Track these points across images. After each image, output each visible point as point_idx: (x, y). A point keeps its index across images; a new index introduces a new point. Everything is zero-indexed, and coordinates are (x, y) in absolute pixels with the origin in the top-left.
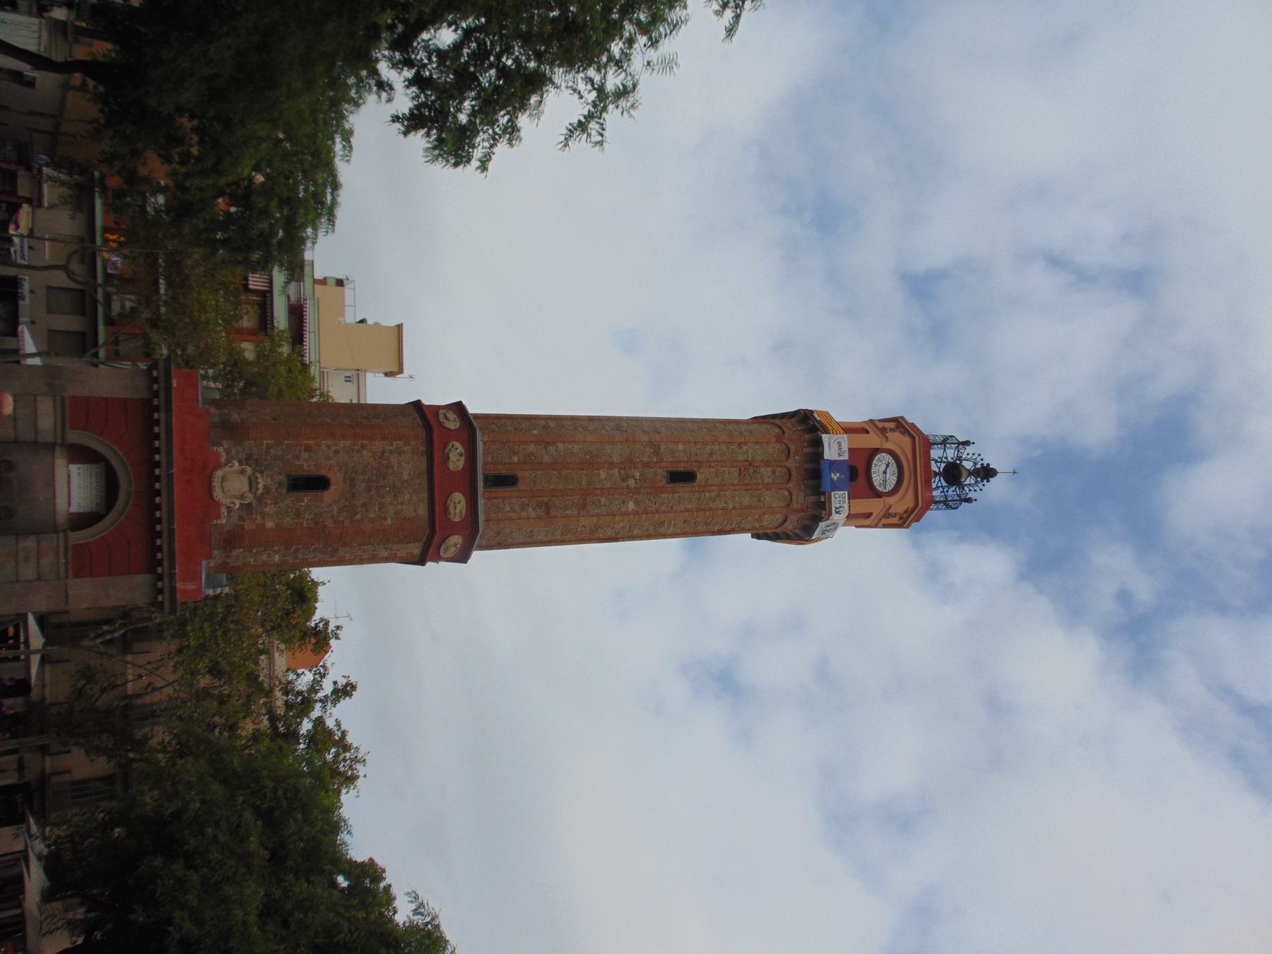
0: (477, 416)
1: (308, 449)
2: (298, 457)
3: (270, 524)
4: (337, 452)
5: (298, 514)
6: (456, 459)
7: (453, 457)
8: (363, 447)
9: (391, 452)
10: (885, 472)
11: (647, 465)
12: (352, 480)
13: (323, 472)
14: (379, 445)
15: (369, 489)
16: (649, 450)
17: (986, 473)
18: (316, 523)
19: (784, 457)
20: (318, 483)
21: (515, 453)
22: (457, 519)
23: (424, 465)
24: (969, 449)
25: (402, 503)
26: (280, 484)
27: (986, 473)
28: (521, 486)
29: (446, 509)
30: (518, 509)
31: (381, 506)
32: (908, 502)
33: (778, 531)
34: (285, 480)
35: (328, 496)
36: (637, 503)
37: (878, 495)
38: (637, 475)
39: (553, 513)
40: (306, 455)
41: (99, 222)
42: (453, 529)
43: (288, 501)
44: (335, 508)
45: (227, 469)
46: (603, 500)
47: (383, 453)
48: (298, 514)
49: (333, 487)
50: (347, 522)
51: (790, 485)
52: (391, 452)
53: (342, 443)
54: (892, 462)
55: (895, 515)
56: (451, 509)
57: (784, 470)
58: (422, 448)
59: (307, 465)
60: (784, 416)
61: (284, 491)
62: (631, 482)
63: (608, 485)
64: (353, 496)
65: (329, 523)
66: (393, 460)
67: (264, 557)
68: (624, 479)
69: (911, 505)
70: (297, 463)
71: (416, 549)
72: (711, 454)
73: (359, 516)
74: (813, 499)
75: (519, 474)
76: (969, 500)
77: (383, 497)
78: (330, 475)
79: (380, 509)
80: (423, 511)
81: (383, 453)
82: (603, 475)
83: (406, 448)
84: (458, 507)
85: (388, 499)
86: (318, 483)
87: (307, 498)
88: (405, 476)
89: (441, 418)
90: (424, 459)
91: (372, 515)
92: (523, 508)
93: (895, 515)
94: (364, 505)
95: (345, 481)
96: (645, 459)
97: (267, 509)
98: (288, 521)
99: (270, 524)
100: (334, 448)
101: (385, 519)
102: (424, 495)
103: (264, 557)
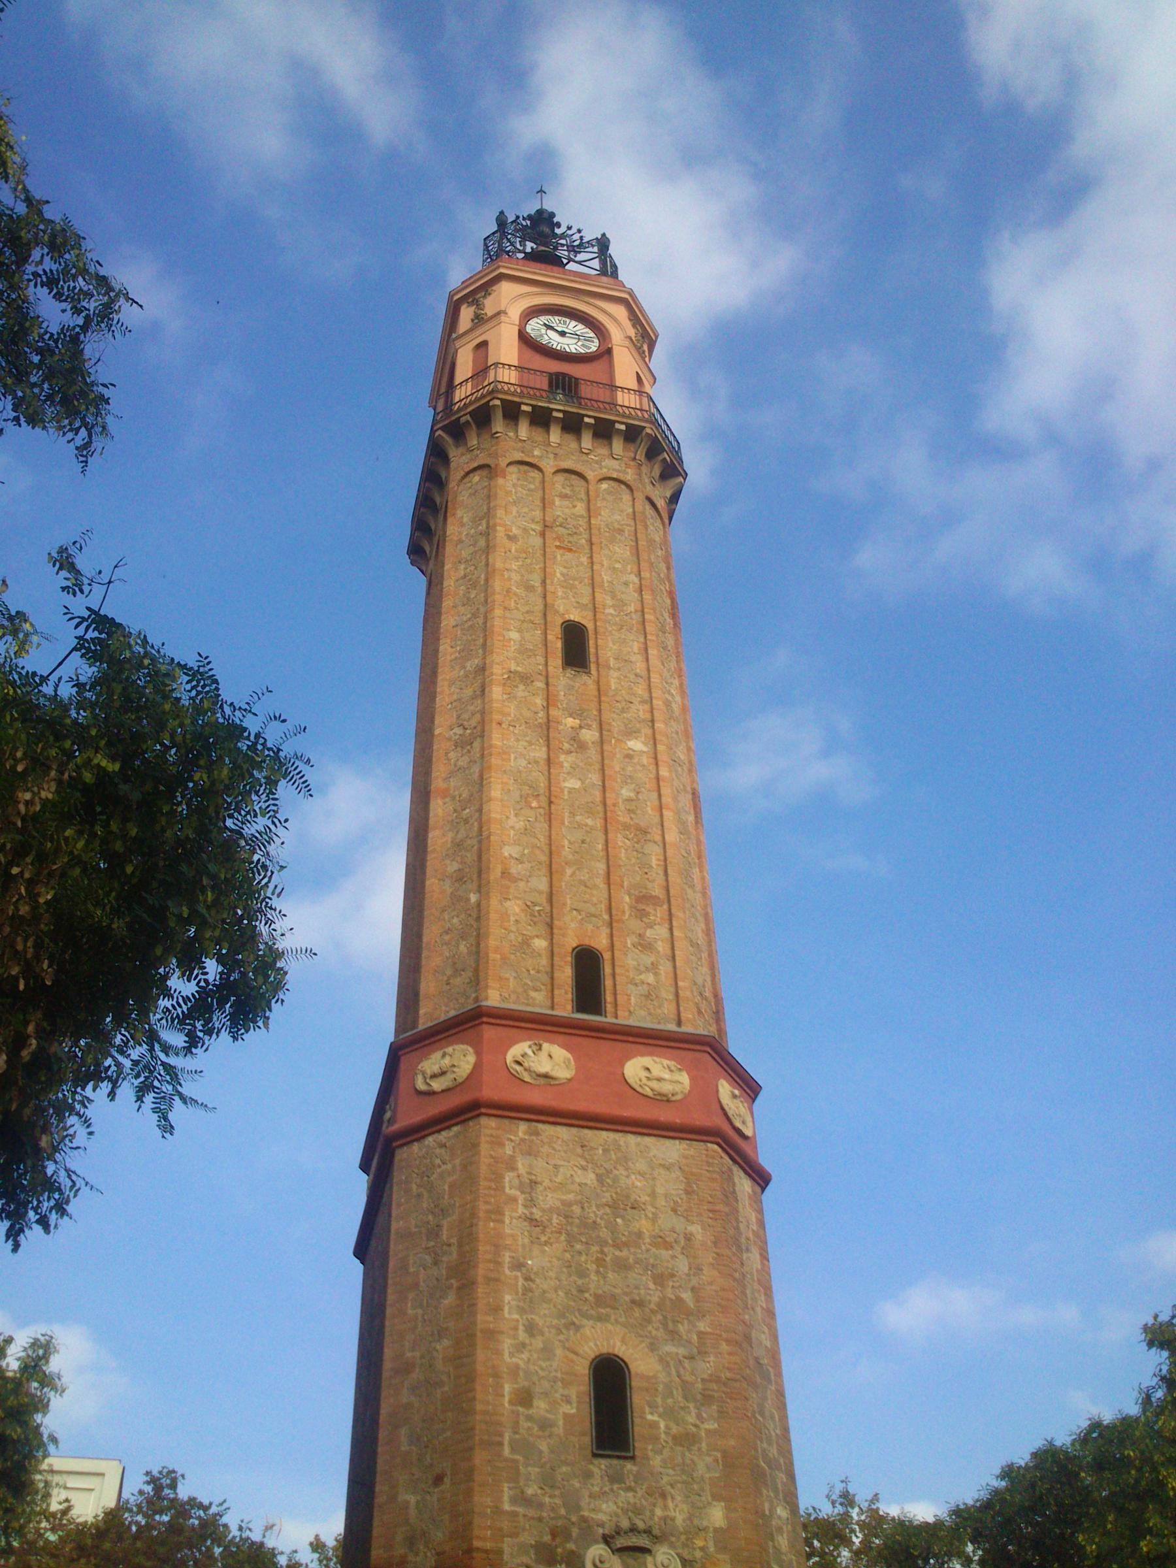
1: (524, 1398)
2: (545, 1425)
3: (717, 1516)
4: (531, 1329)
6: (552, 1060)
7: (544, 1066)
8: (518, 1265)
9: (531, 1202)
10: (563, 334)
11: (549, 701)
12: (600, 1300)
13: (583, 1369)
14: (512, 1225)
15: (622, 1266)
16: (521, 691)
18: (707, 1399)
19: (535, 474)
21: (526, 942)
22: (685, 1078)
23: (563, 1132)
25: (653, 1194)
26: (615, 1478)
28: (600, 942)
29: (663, 1099)
30: (648, 959)
31: (661, 1242)
32: (620, 312)
34: (604, 1463)
35: (642, 1364)
36: (631, 733)
37: (606, 353)
38: (570, 722)
39: (657, 891)
40: (540, 1406)
42: (704, 1092)
43: (656, 1462)
44: (669, 1348)
46: (626, 793)
47: (532, 1221)
48: (687, 1440)
49: (620, 1349)
50: (702, 1326)
51: (590, 475)
52: (531, 1202)
53: (510, 1314)
54: (544, 319)
56: (666, 1088)
57: (560, 478)
58: (523, 1127)
59: (570, 1405)
61: (629, 1466)
62: (589, 735)
63: (595, 778)
64: (640, 1304)
65: (707, 1366)
66: (549, 1199)
68: (582, 746)
70: (559, 1429)
71: (744, 1185)
72: (530, 588)
73: (687, 1296)
74: (618, 445)
75: (572, 942)
76: (603, 244)
77: (640, 1234)
79: (668, 1246)
80: (672, 1150)
81: (532, 1221)
82: (573, 783)
83: (521, 1164)
84: (657, 1071)
85: (644, 1225)
87: (648, 1415)
88: (590, 1178)
90: (547, 1130)
91: (682, 1265)
92: (646, 946)
94: (659, 1280)
95: (600, 1319)
96: (539, 701)
97: (680, 1519)
98: (705, 1466)
99: (717, 1516)
100: (522, 1335)
101: (688, 1238)
102: (631, 1142)
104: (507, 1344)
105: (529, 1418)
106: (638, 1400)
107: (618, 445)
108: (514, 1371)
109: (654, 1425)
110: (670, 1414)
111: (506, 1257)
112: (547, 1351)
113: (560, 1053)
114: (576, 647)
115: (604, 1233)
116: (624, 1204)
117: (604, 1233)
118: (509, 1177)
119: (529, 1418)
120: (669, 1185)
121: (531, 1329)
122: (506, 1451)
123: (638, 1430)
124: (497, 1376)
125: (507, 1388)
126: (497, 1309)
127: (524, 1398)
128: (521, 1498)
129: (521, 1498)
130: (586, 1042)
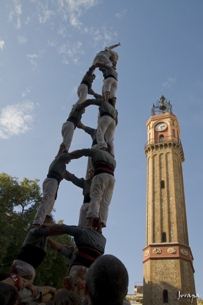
1: (155, 296)
2: (158, 299)
13: (162, 291)
14: (154, 274)
17: (163, 98)
23: (160, 260)
24: (155, 105)
27: (163, 98)
40: (157, 297)
49: (167, 289)
59: (160, 296)
70: (159, 300)
80: (173, 261)
87: (170, 296)
89: (147, 255)
102: (168, 260)
104: (153, 289)
105: (156, 298)
109: (171, 298)
118: (153, 267)
119: (156, 298)
122: (153, 303)
123: (169, 299)
124: (152, 293)
125: (153, 295)
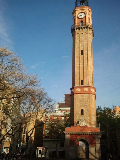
0: (72, 86)
1: (77, 112)
3: (88, 118)
4: (77, 108)
5: (87, 114)
7: (78, 90)
9: (77, 100)
13: (81, 110)
20: (82, 111)
22: (88, 89)
23: (80, 95)
26: (82, 116)
28: (83, 79)
33: (92, 34)
35: (84, 109)
40: (78, 113)
41: (50, 140)
43: (85, 115)
45: (80, 124)
47: (78, 101)
48: (87, 114)
52: (77, 100)
55: (89, 13)
59: (80, 112)
60: (72, 35)
67: (94, 119)
69: (87, 10)
73: (87, 105)
75: (81, 80)
78: (81, 109)
81: (78, 101)
85: (85, 100)
86: (82, 111)
87: (84, 112)
93: (89, 13)
94: (86, 104)
99: (88, 118)
101: (88, 101)
103: (94, 119)
104: (76, 109)
106: (84, 112)
107: (86, 29)
108: (76, 111)
110: (86, 112)
111: (76, 104)
112: (78, 109)
113: (79, 89)
114: (82, 53)
115: (82, 101)
116: (83, 99)
117: (82, 101)
120: (87, 97)
121: (77, 108)
123: (84, 113)
126: (75, 107)
127: (77, 112)
128: (77, 118)
129: (77, 118)
130: (82, 88)
